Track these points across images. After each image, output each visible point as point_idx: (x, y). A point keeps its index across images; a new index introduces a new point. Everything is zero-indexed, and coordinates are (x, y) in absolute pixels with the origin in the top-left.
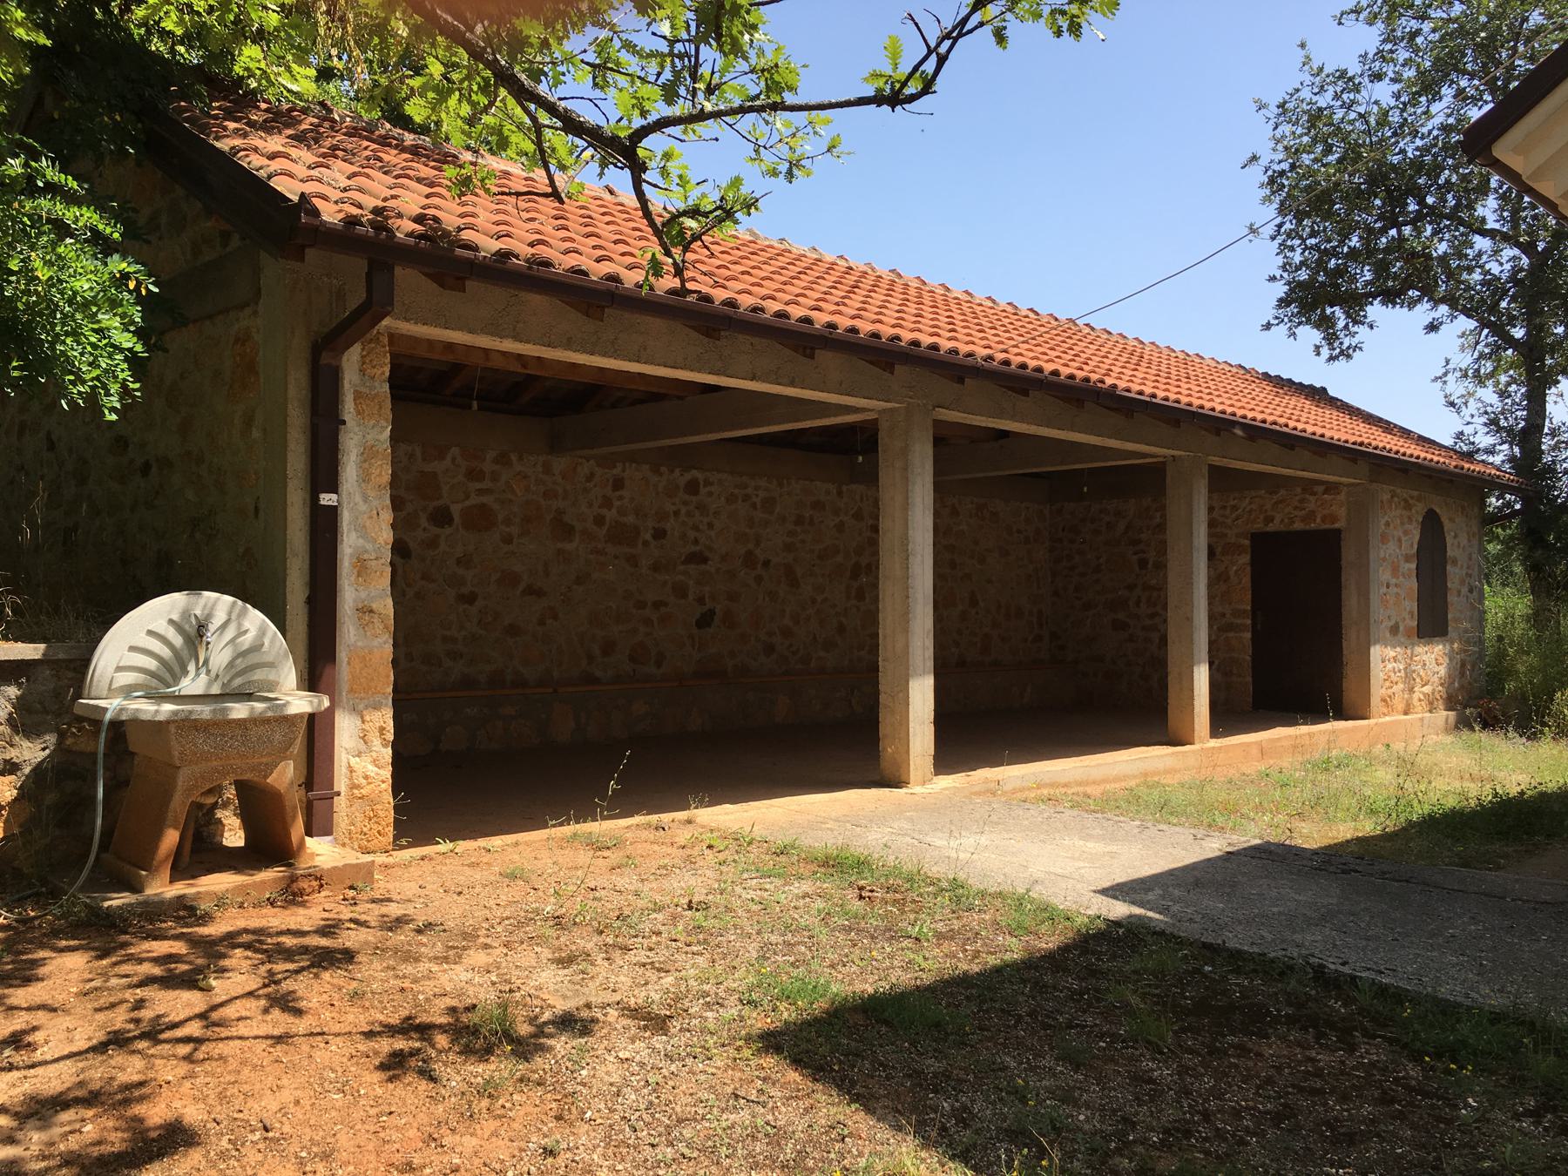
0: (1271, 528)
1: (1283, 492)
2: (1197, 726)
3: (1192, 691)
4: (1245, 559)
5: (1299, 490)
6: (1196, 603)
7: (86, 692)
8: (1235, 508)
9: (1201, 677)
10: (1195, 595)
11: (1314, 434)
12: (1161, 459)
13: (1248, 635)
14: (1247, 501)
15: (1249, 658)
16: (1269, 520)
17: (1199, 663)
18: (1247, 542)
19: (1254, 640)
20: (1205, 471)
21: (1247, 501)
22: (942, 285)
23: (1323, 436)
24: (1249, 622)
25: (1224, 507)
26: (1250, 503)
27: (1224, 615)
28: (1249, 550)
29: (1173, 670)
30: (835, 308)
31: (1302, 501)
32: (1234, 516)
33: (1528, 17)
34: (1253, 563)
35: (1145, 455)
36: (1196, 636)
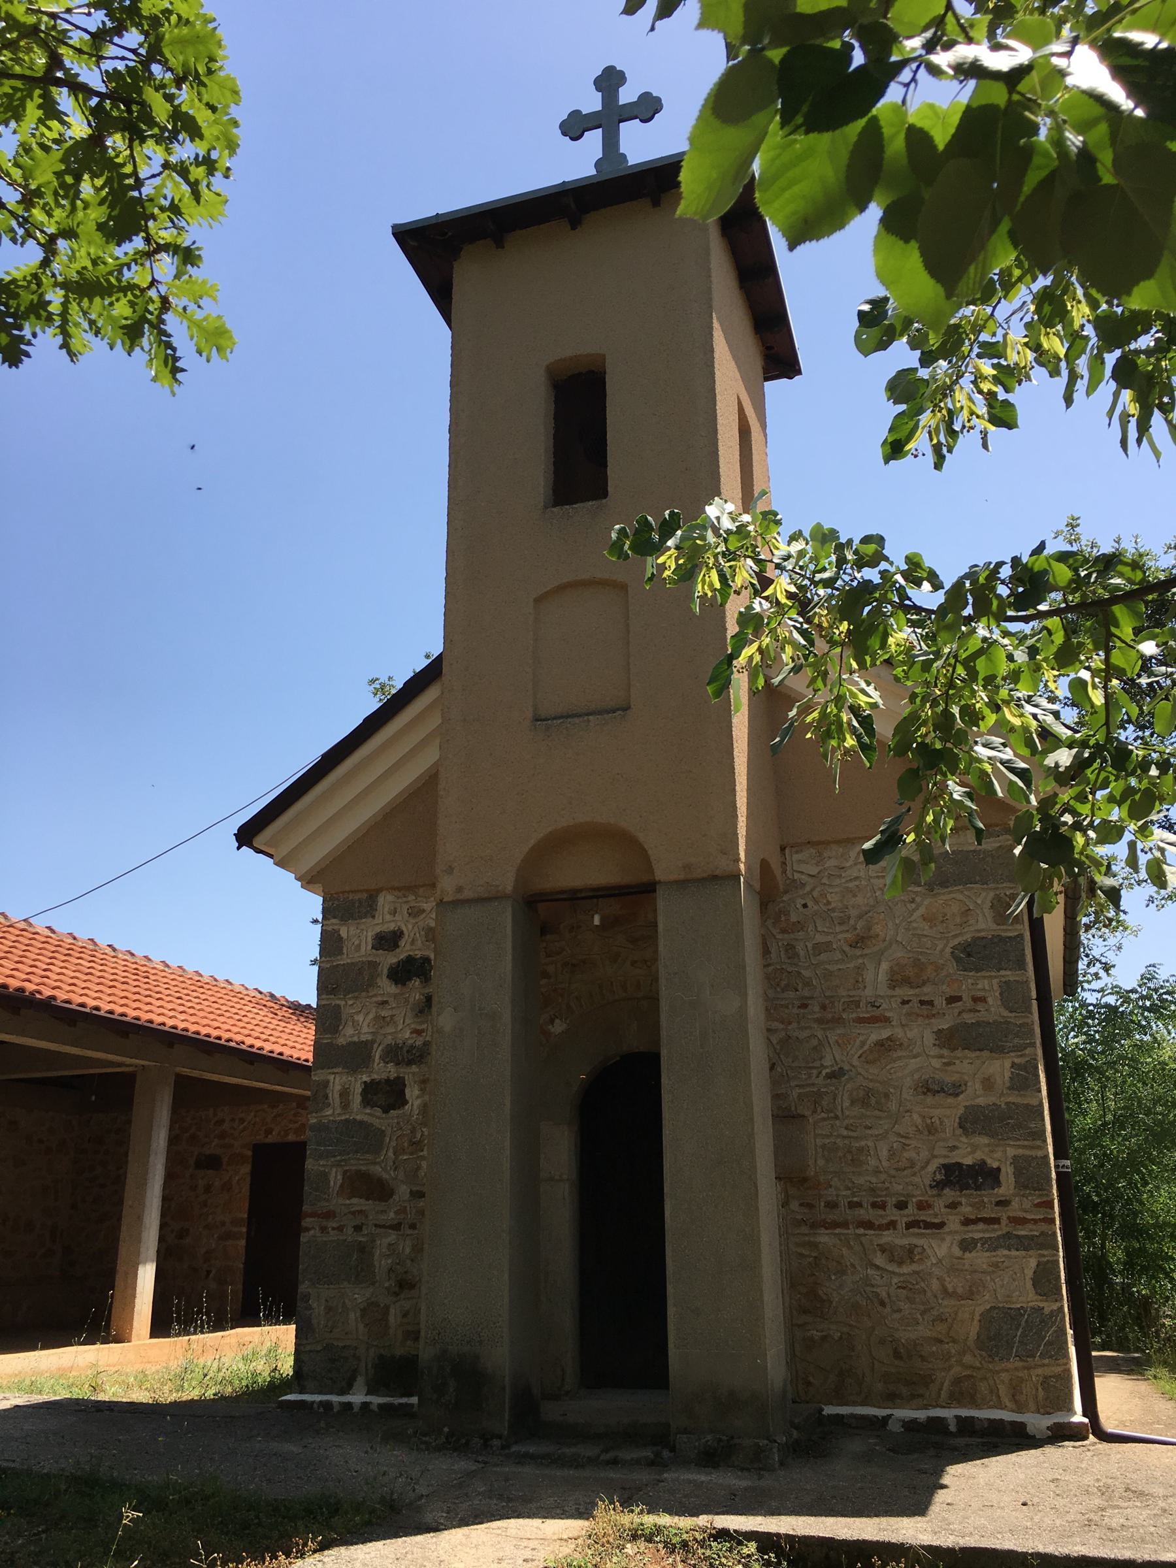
0: (270, 1139)
1: (281, 1106)
2: (135, 1324)
3: (135, 1288)
4: (246, 1169)
5: (294, 1104)
6: (148, 1204)
7: (108, 1327)
8: (242, 1120)
9: (146, 1277)
10: (148, 1194)
11: (272, 1052)
12: (131, 1069)
13: (243, 1242)
14: (252, 1114)
15: (242, 1266)
16: (269, 1132)
17: (145, 1263)
18: (250, 1153)
19: (247, 1247)
20: (172, 1080)
21: (252, 1114)
22: (70, 934)
23: (281, 1054)
24: (244, 1230)
25: (233, 1120)
26: (255, 1116)
27: (223, 1224)
28: (251, 1160)
29: (121, 1268)
30: (18, 959)
31: (295, 1115)
32: (241, 1127)
33: (826, 670)
34: (254, 1174)
35: (120, 1065)
36: (145, 1235)
